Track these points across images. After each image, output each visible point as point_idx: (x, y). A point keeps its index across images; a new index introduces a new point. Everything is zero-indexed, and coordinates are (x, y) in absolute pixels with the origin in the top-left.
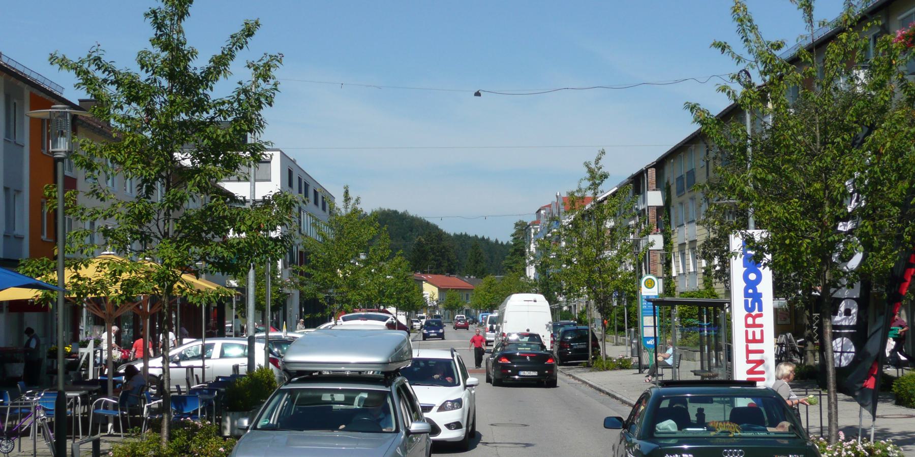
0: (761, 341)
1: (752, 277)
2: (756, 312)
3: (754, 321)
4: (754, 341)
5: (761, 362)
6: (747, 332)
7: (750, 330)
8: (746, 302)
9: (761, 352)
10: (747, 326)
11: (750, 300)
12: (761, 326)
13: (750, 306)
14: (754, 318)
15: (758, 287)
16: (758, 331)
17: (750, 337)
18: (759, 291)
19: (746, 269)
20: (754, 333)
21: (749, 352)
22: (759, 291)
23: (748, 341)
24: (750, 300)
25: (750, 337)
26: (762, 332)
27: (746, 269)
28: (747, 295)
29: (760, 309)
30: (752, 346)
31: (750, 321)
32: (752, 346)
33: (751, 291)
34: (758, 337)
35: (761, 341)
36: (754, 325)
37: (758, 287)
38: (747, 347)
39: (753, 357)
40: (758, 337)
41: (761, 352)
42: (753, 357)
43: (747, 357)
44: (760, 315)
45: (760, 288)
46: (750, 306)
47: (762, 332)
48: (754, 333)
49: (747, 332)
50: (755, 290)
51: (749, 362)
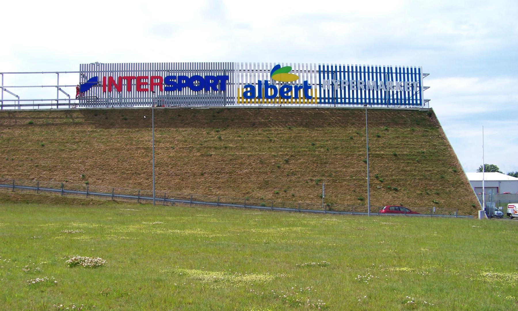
0: (139, 89)
1: (196, 83)
3: (157, 84)
8: (174, 77)
10: (152, 78)
14: (160, 84)
20: (146, 84)
23: (139, 79)
26: (146, 90)
28: (181, 78)
29: (167, 89)
30: (134, 82)
31: (157, 81)
32: (134, 82)
36: (152, 84)
38: (134, 78)
39: (125, 82)
42: (125, 82)
43: (125, 78)
44: (161, 90)
47: (146, 90)
48: (146, 84)
49: (147, 78)
50: (185, 86)
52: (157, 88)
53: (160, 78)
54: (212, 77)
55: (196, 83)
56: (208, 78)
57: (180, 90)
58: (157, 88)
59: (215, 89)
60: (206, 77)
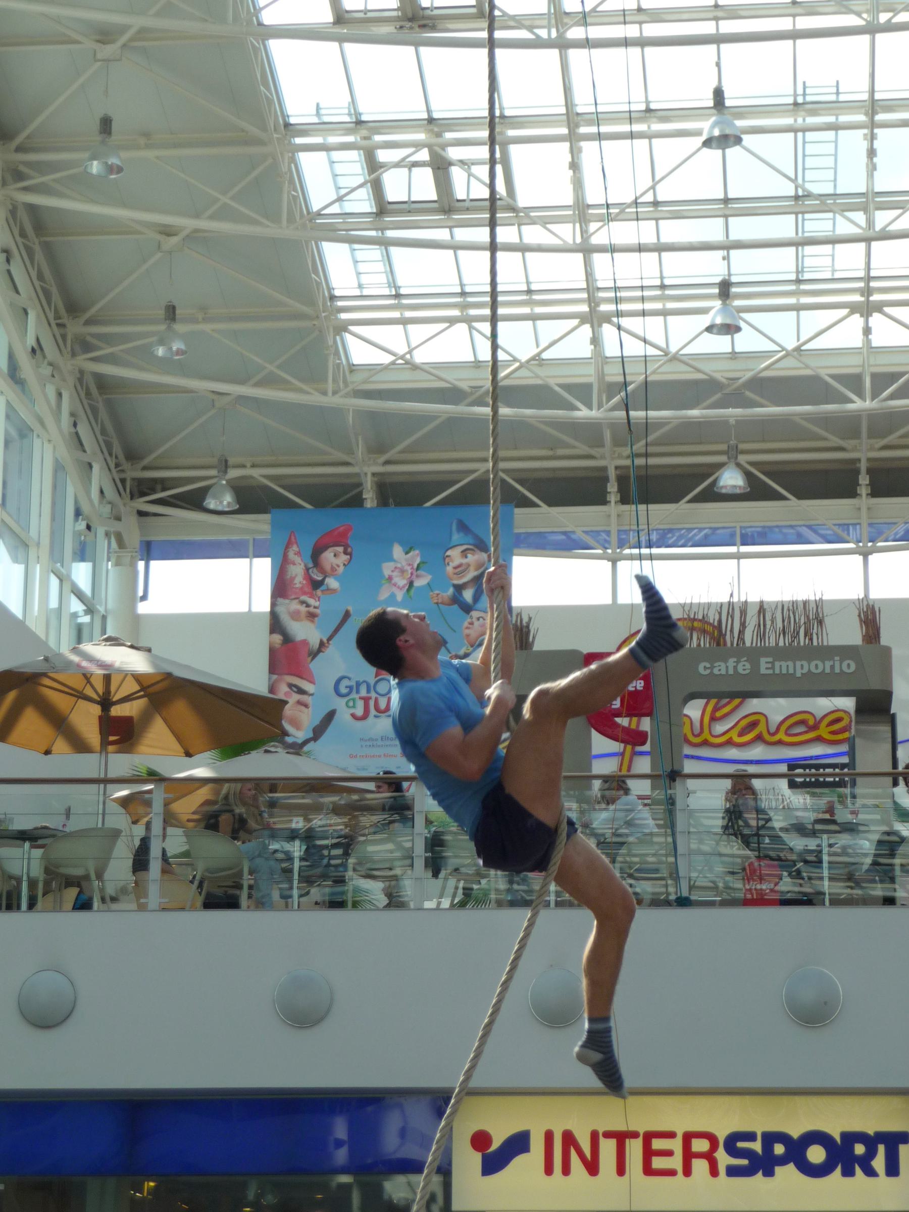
0: (648, 1170)
1: (816, 1154)
2: (724, 1159)
4: (649, 1153)
5: (592, 1167)
6: (671, 1135)
7: (676, 1145)
8: (751, 1137)
9: (621, 1170)
10: (688, 1138)
11: (757, 1146)
12: (687, 1172)
13: (740, 1145)
14: (709, 1157)
15: (791, 1167)
16: (676, 1163)
17: (657, 1144)
18: (778, 1170)
19: (838, 1139)
20: (669, 1153)
21: (621, 1138)
23: (649, 1137)
24: (757, 1146)
25: (657, 1144)
26: (672, 1173)
27: (838, 1139)
28: (770, 1138)
29: (732, 1171)
30: (635, 1148)
32: (635, 1148)
33: (779, 1149)
34: (658, 1163)
35: (648, 1170)
36: (688, 1156)
37: (791, 1167)
38: (635, 1135)
39: (608, 1148)
40: (658, 1163)
41: (621, 1171)
42: (608, 1148)
43: (608, 1135)
44: (714, 1172)
45: (787, 1173)
46: (740, 1145)
47: (672, 1173)
48: (669, 1153)
49: (671, 1135)
50: (783, 1161)
51: (594, 1136)
52: (700, 1166)
53: (711, 1138)
55: (816, 1154)
56: (850, 1138)
57: (769, 1173)
58: (700, 1166)
59: (870, 1172)
60: (845, 1136)
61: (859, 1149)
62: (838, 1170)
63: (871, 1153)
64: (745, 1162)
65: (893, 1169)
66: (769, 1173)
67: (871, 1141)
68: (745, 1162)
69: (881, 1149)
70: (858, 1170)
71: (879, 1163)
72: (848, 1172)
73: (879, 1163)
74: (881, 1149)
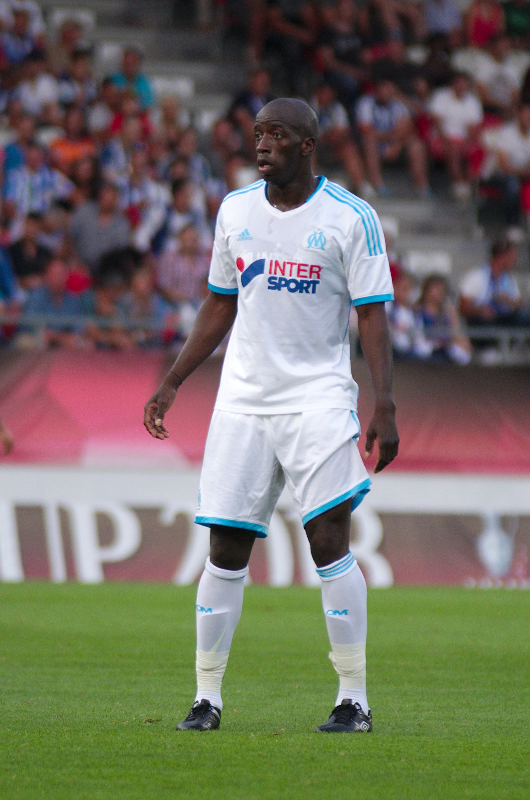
1: (293, 286)
11: (277, 281)
13: (273, 281)
18: (282, 288)
22: (282, 288)
24: (277, 281)
33: (283, 283)
45: (285, 289)
50: (284, 286)
54: (306, 282)
55: (293, 286)
57: (279, 289)
59: (307, 292)
61: (305, 285)
62: (299, 291)
63: (308, 286)
64: (273, 285)
65: (314, 291)
66: (279, 289)
67: (309, 283)
68: (273, 285)
69: (312, 285)
70: (304, 291)
71: (310, 290)
72: (301, 292)
73: (310, 290)
74: (312, 285)
